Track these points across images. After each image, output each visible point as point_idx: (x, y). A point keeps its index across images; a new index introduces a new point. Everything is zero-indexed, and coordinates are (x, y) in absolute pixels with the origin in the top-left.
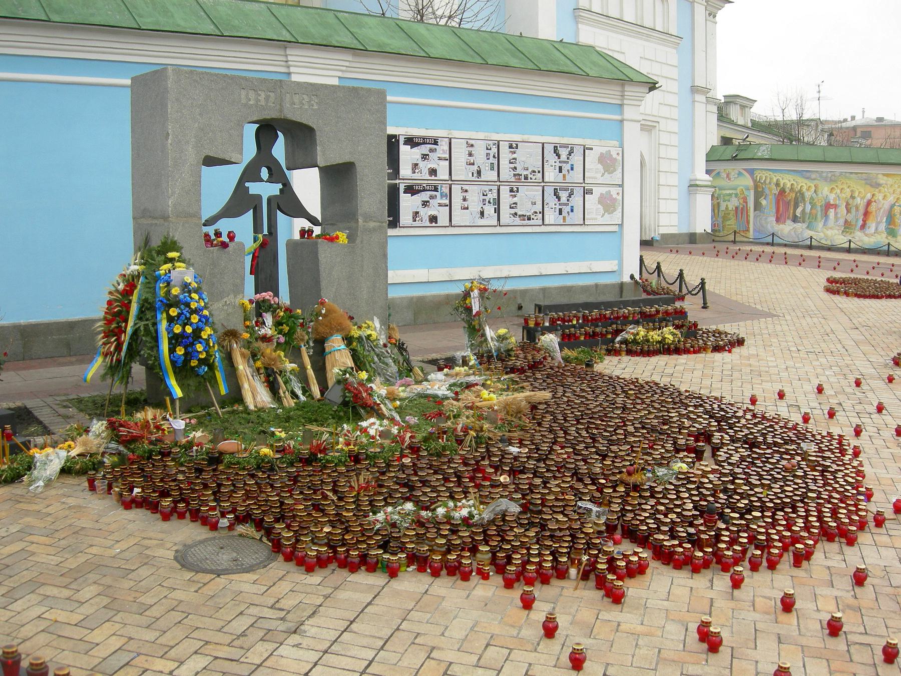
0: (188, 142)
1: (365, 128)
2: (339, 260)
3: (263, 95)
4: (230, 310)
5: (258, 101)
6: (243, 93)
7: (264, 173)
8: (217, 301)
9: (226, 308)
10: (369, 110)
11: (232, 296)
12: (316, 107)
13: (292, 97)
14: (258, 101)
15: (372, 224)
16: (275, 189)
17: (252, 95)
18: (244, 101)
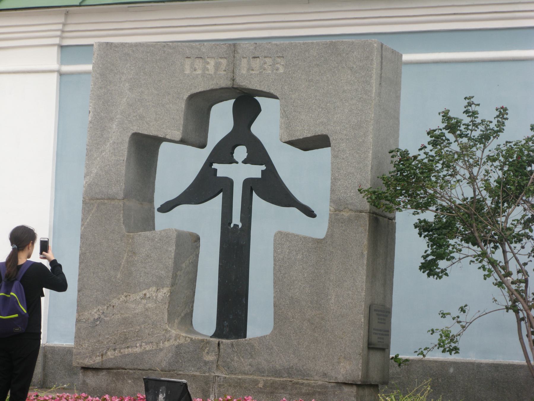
0: (112, 119)
1: (344, 91)
2: (299, 257)
3: (212, 62)
4: (150, 305)
5: (205, 69)
6: (188, 62)
7: (241, 153)
8: (135, 293)
9: (144, 301)
10: (351, 69)
11: (154, 289)
12: (281, 70)
13: (249, 62)
14: (205, 69)
15: (346, 214)
16: (256, 171)
17: (199, 64)
18: (187, 72)
